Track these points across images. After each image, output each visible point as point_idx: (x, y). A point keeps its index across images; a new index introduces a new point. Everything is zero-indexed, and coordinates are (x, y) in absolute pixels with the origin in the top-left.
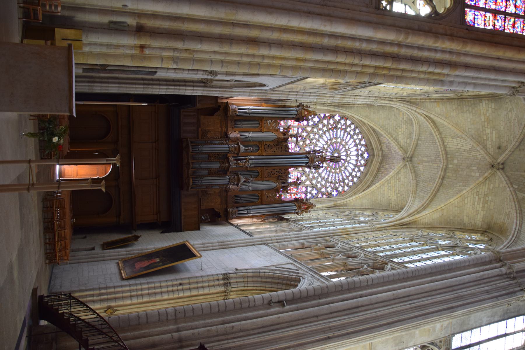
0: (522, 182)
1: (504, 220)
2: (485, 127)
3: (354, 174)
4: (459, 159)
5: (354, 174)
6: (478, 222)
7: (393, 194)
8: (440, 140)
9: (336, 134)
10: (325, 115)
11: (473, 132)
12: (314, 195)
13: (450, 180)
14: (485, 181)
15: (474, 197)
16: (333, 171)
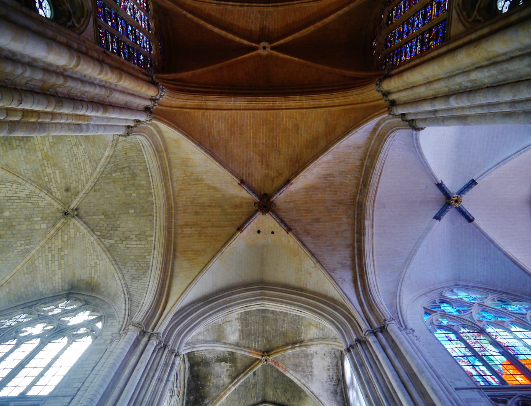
0: (103, 227)
1: (91, 273)
2: (45, 166)
4: (11, 210)
6: (57, 284)
11: (30, 174)
13: (4, 240)
14: (57, 233)
15: (45, 256)
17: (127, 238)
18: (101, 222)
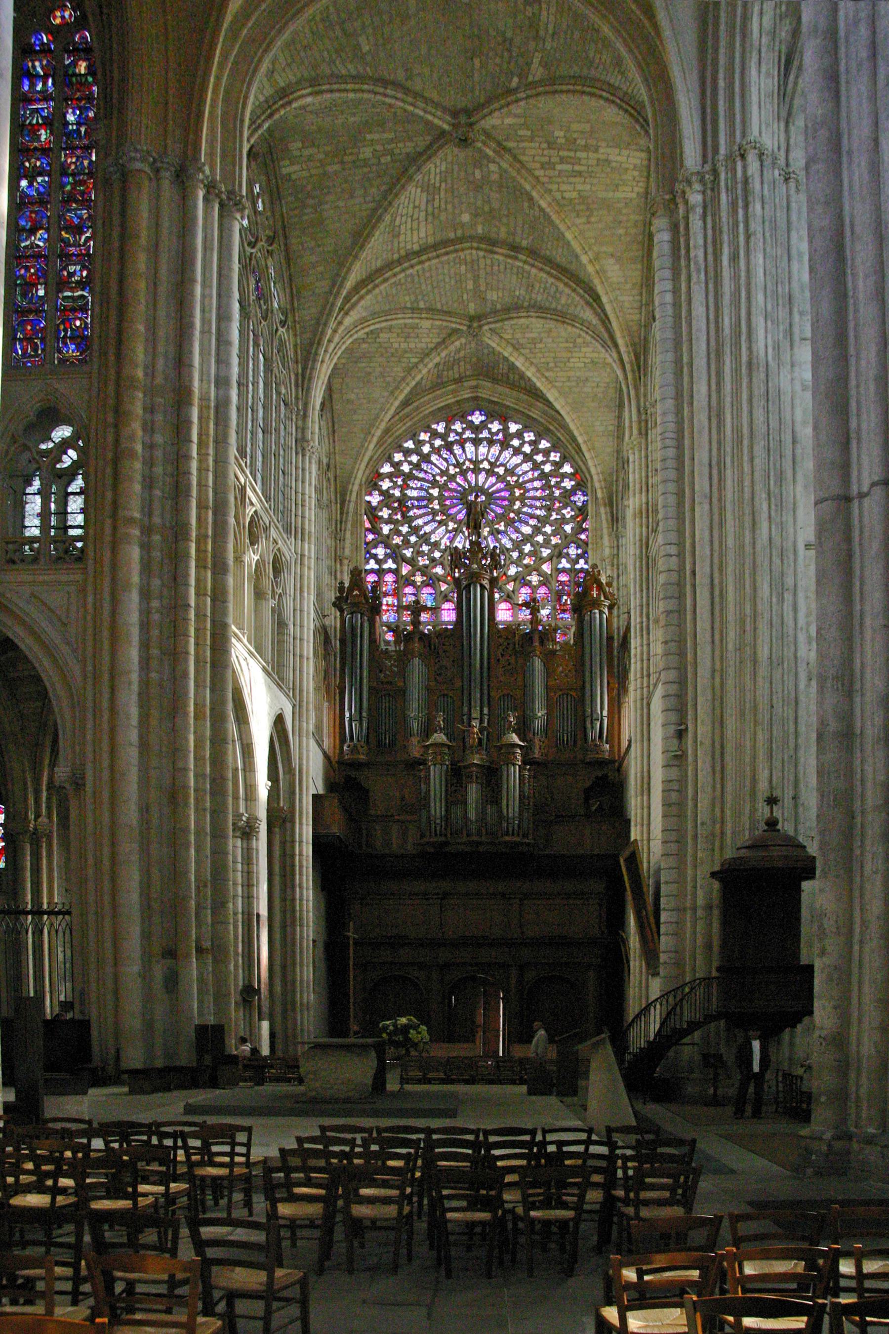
5: (527, 449)
7: (577, 355)
8: (406, 265)
9: (418, 499)
10: (368, 530)
12: (580, 551)
13: (519, 230)
14: (509, 151)
16: (518, 504)
17: (533, 23)
18: (490, 67)
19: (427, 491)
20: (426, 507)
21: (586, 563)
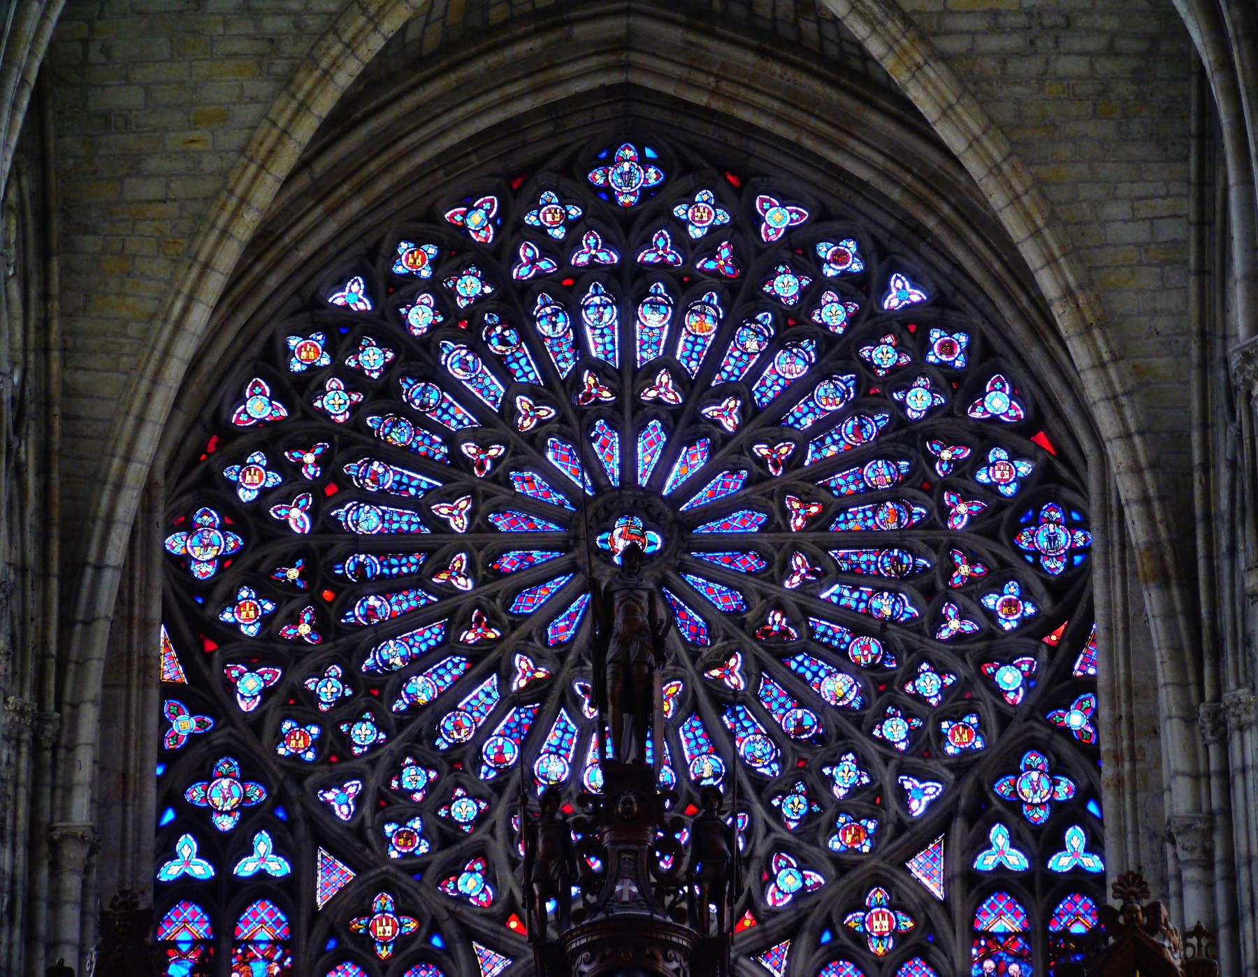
3: (833, 314)
9: (383, 545)
10: (170, 690)
19: (420, 506)
20: (416, 582)
21: (1094, 846)
